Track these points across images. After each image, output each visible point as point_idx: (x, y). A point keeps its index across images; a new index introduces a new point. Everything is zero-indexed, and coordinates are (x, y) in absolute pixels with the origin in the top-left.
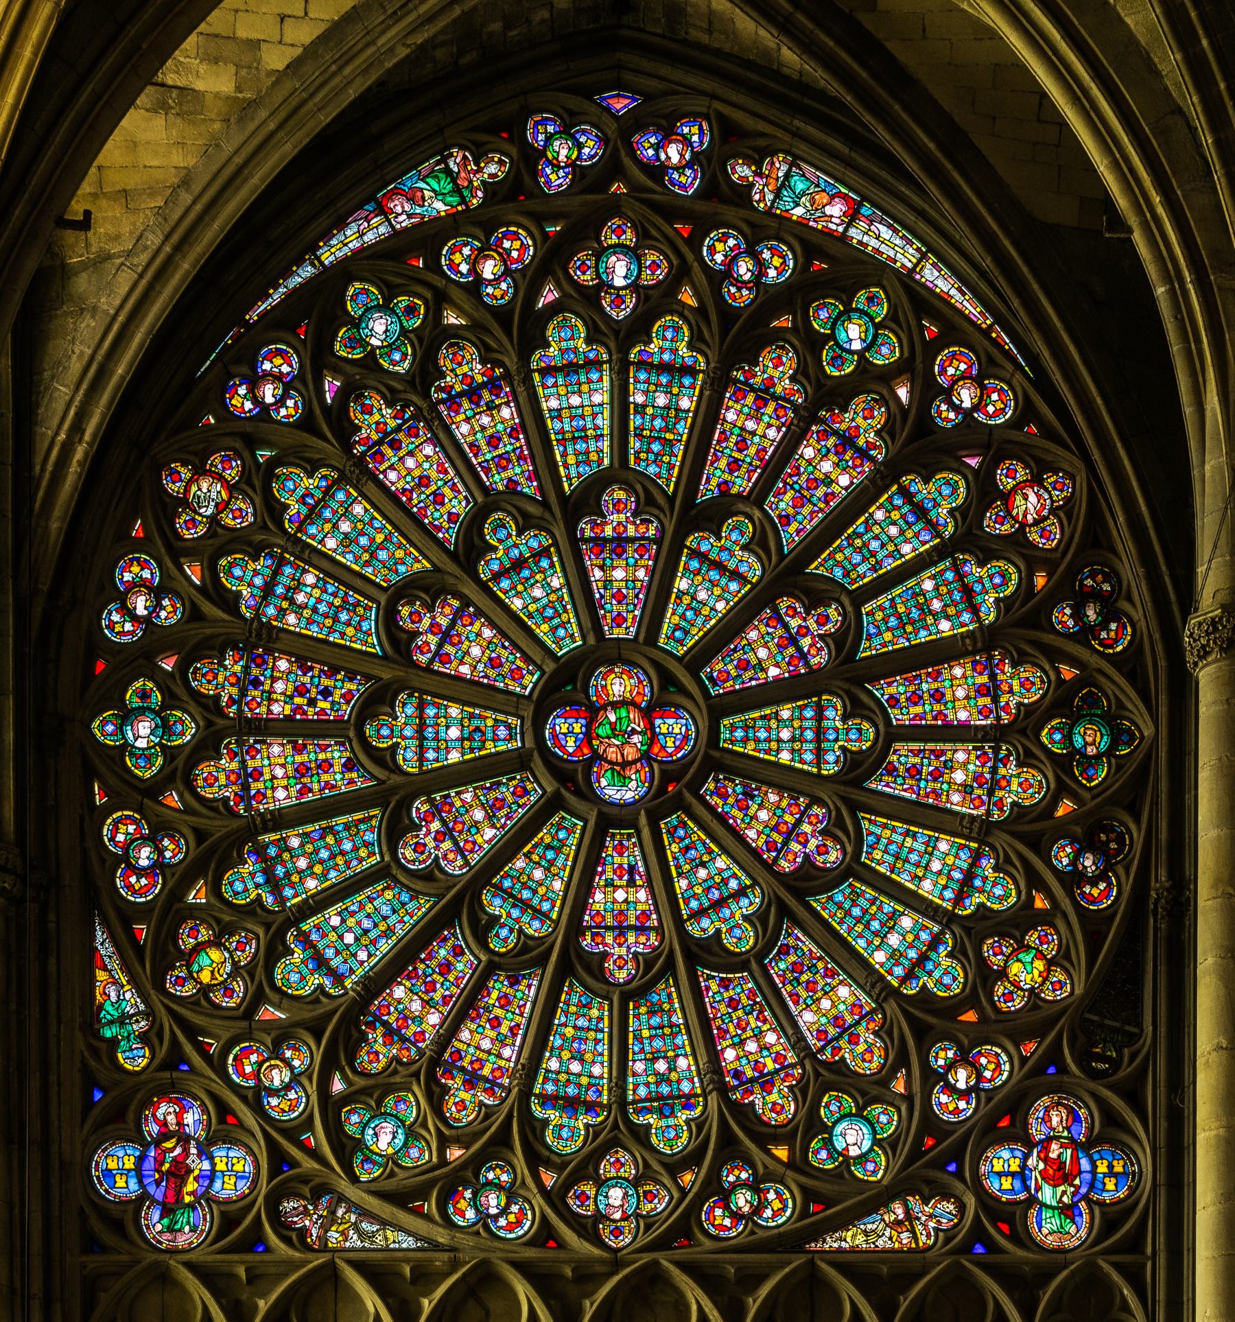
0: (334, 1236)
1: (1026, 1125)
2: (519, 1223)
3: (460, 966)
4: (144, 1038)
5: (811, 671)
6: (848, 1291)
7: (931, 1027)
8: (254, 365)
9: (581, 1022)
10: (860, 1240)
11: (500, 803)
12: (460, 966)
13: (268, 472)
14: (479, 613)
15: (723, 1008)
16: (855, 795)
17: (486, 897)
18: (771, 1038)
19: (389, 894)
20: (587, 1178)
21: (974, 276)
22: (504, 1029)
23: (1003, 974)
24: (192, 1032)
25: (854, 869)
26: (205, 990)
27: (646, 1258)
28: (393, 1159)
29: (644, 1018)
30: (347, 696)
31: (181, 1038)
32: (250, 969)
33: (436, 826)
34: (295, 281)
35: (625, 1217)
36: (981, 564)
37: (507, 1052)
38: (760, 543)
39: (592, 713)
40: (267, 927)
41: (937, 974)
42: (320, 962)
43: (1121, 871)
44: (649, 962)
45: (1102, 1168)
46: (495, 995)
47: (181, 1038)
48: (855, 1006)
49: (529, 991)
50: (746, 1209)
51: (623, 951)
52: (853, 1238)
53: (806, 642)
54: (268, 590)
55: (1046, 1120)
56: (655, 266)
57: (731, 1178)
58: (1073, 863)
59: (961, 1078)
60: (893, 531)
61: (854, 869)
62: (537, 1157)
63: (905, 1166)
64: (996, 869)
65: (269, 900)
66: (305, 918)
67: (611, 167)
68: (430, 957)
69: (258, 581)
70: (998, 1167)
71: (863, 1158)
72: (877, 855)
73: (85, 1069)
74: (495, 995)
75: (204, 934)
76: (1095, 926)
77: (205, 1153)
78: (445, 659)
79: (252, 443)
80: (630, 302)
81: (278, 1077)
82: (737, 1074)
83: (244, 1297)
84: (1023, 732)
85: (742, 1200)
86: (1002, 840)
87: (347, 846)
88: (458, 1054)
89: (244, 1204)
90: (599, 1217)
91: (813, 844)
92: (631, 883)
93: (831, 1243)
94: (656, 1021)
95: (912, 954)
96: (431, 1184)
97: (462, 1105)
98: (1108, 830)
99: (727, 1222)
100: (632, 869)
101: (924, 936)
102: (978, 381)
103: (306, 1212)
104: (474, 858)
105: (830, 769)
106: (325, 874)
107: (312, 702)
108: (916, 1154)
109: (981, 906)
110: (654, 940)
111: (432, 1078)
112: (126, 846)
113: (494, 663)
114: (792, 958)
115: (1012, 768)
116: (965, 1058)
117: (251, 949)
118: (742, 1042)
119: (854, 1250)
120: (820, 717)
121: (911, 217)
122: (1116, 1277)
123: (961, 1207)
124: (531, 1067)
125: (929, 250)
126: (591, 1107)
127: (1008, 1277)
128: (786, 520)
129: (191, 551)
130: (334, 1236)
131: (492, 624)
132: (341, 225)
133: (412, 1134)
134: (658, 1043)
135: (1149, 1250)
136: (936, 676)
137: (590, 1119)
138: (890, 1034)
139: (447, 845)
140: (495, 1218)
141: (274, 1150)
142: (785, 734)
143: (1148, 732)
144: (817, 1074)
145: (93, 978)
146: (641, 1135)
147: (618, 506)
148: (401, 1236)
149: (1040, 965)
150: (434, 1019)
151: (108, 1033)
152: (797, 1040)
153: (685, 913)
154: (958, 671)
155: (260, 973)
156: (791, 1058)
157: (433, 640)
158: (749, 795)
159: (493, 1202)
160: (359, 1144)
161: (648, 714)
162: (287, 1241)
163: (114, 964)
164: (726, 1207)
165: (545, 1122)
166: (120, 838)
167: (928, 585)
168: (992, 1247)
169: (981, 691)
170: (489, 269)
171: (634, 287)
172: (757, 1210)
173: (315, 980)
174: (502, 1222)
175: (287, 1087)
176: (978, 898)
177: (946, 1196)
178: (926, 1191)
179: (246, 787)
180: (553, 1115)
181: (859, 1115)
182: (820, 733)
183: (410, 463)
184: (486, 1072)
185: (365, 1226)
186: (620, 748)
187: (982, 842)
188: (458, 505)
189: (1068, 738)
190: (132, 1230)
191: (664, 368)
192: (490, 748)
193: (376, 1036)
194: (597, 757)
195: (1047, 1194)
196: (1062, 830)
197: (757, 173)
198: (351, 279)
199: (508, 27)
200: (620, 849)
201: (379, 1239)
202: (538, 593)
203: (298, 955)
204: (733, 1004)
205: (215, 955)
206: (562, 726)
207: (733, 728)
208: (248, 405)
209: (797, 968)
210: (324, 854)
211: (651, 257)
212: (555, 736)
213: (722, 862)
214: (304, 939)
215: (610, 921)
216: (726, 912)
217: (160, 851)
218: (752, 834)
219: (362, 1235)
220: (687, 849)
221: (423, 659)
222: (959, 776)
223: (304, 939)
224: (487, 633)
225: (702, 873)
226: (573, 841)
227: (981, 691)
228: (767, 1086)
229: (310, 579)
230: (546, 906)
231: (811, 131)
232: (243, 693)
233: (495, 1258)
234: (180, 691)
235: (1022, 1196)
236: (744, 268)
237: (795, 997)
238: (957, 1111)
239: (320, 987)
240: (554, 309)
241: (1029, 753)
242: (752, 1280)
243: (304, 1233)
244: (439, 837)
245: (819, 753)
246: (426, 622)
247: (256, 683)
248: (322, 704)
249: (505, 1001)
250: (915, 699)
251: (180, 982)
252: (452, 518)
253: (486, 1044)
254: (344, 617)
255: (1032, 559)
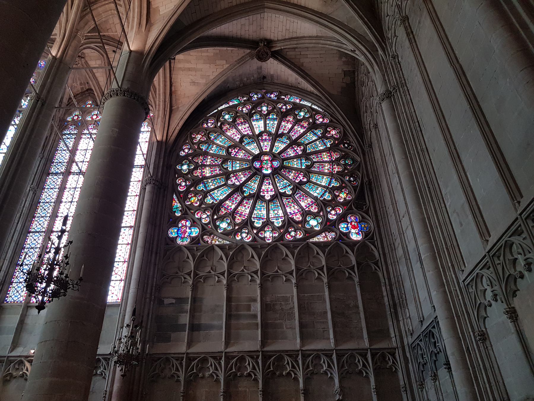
0: (213, 242)
1: (347, 219)
2: (249, 238)
3: (239, 198)
4: (181, 211)
5: (299, 154)
6: (315, 248)
7: (326, 204)
8: (207, 121)
9: (261, 206)
10: (317, 240)
11: (246, 174)
12: (239, 198)
13: (209, 134)
14: (242, 149)
15: (287, 203)
16: (308, 170)
17: (243, 187)
18: (296, 207)
19: (226, 188)
20: (263, 230)
21: (320, 106)
22: (247, 207)
23: (339, 196)
24: (190, 209)
25: (309, 181)
26: (192, 203)
27: (275, 243)
28: (225, 229)
29: (272, 205)
30: (220, 161)
31: (187, 210)
32: (201, 199)
33: (235, 178)
34: (214, 112)
35: (270, 237)
36: (326, 140)
37: (246, 211)
38: (289, 138)
39: (261, 162)
40: (204, 193)
41: (326, 196)
42: (213, 198)
43: (358, 179)
44: (273, 196)
45: (363, 226)
46: (245, 202)
47: (187, 210)
48: (312, 202)
49: (251, 202)
50: (294, 235)
51: (268, 195)
52: (315, 239)
53: (298, 151)
54: (208, 148)
55: (351, 218)
56: (270, 108)
57: (291, 230)
58: (349, 179)
59: (333, 212)
60: (311, 136)
61: (309, 181)
62: (253, 227)
63: (324, 226)
64: (335, 180)
65: (204, 189)
66: (211, 192)
67: (263, 97)
68: (233, 197)
69: (206, 147)
70: (342, 226)
71: (316, 226)
72: (313, 179)
73: (169, 215)
74: (245, 202)
75: (193, 195)
76: (355, 188)
77: (190, 228)
78: (237, 155)
79: (206, 130)
80: (266, 112)
81: (204, 216)
82: (290, 213)
83: (195, 253)
84: (337, 161)
85: (293, 234)
86: (335, 176)
87: (219, 181)
88: (238, 211)
89: (197, 237)
90: (265, 237)
91: (301, 178)
92: (269, 185)
93: (311, 240)
94: (274, 205)
95: (322, 193)
96: (233, 232)
97: (238, 219)
98: (355, 174)
99: (290, 237)
100: (269, 183)
101: (323, 191)
102: (323, 118)
103: (209, 238)
104: (241, 182)
105: (303, 167)
106: (215, 185)
107: (214, 162)
108: (326, 225)
109: (333, 186)
110: (273, 193)
111: (233, 215)
112: (180, 183)
113: (245, 156)
114: (299, 195)
115: (336, 166)
116: (333, 209)
117: (201, 197)
118: (291, 208)
119: (316, 241)
120: (301, 160)
121: (310, 100)
122: (369, 244)
123: (336, 234)
124: (251, 213)
125: (313, 104)
126: (263, 219)
127: (348, 245)
128: (293, 136)
129: (195, 144)
130: (213, 242)
131: (244, 151)
132: (222, 105)
133: (229, 224)
134: (275, 208)
135: (375, 239)
136: (321, 154)
137: (263, 221)
138: (319, 205)
139: (237, 180)
140: (245, 238)
141: (202, 226)
142: (295, 163)
143: (359, 160)
144: (306, 212)
145: (172, 202)
146: (273, 223)
147: (265, 135)
148: (226, 241)
149: (345, 194)
150: (233, 207)
151: (174, 210)
152: (301, 207)
153: (279, 189)
154: (324, 154)
155: (202, 200)
156: (300, 210)
157: (235, 153)
158: (289, 172)
159: (244, 235)
160: (219, 226)
161: (271, 161)
162: (205, 242)
163: (176, 200)
164: (290, 235)
165: (254, 221)
166: (180, 181)
167: (318, 143)
168: (343, 239)
169: (329, 156)
170: (244, 109)
171: (267, 110)
172: (296, 235)
173: (212, 201)
174: (246, 238)
175: (206, 218)
176: (332, 185)
177: (333, 232)
178: (329, 230)
179: (202, 174)
180: (256, 221)
181: (314, 218)
182: (301, 163)
183: (231, 132)
184: (243, 214)
185: (220, 240)
186: (267, 166)
187: (332, 177)
188: (239, 137)
189: (345, 162)
190: (175, 241)
191: (272, 119)
192: (244, 167)
193: (223, 210)
194: (262, 167)
195: (353, 231)
196: (346, 175)
197: (286, 97)
198: (223, 111)
199: (247, 80)
200: (267, 180)
201: (222, 242)
202: (252, 146)
203: (209, 197)
204: (289, 202)
205: (195, 198)
206: (257, 163)
207: (286, 163)
208: (206, 126)
209: (300, 196)
210: (215, 183)
211: (269, 107)
212: (255, 165)
213: (285, 181)
214: (211, 195)
215: (266, 190)
216: (286, 189)
217: (186, 183)
218: (290, 177)
219: (219, 242)
220: (279, 180)
221: (233, 156)
222: (326, 168)
223: (211, 195)
224: (244, 152)
225: (282, 183)
226: (259, 179)
227: (329, 156)
228: (296, 215)
229: (215, 146)
230: (254, 189)
231: (293, 91)
232: (202, 161)
233: (245, 244)
234: (192, 161)
235: (348, 231)
236: (284, 107)
237: (300, 201)
238: (333, 218)
239: (213, 202)
240: (254, 113)
241: (338, 164)
242: (296, 247)
243: (208, 241)
244: (235, 179)
245: (301, 165)
246: (234, 151)
247: (205, 160)
248: (216, 162)
249: (247, 203)
250: (317, 157)
251: (188, 202)
252: (238, 138)
253: (243, 210)
254: (220, 151)
255: (335, 139)
